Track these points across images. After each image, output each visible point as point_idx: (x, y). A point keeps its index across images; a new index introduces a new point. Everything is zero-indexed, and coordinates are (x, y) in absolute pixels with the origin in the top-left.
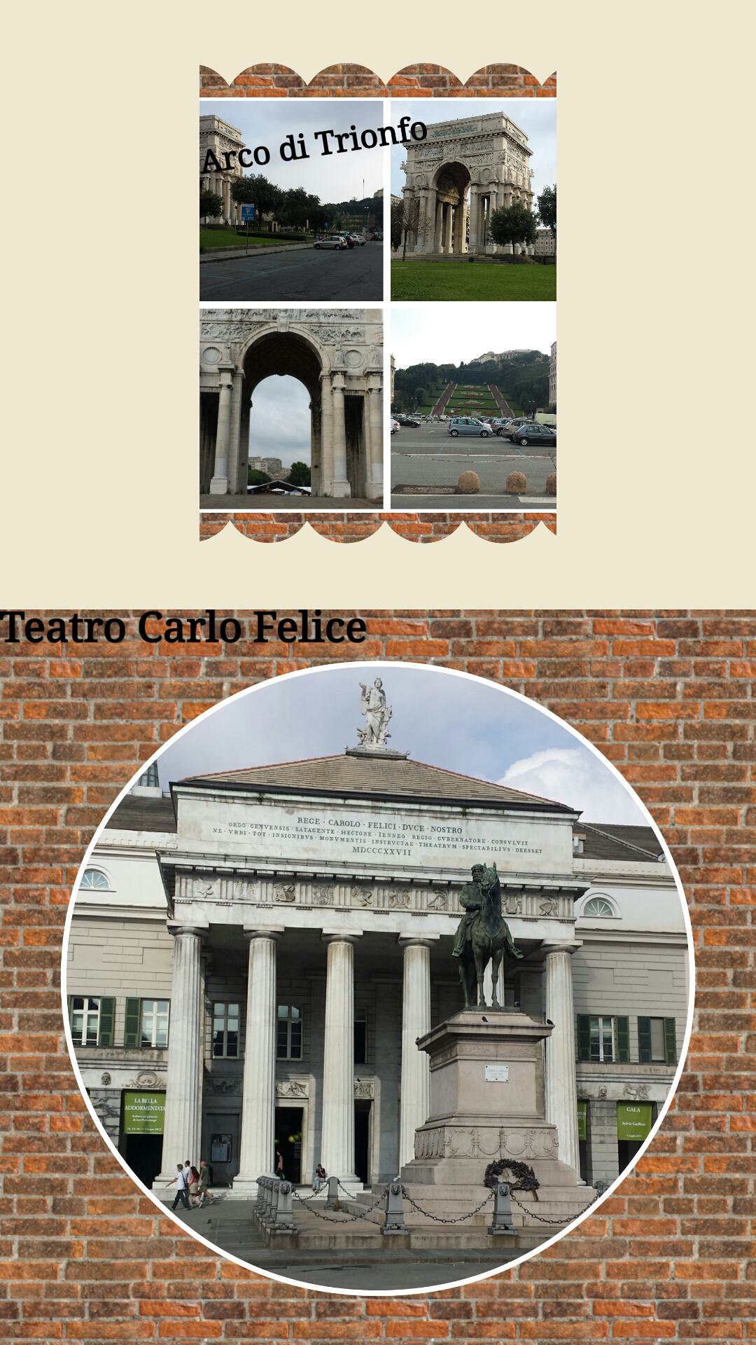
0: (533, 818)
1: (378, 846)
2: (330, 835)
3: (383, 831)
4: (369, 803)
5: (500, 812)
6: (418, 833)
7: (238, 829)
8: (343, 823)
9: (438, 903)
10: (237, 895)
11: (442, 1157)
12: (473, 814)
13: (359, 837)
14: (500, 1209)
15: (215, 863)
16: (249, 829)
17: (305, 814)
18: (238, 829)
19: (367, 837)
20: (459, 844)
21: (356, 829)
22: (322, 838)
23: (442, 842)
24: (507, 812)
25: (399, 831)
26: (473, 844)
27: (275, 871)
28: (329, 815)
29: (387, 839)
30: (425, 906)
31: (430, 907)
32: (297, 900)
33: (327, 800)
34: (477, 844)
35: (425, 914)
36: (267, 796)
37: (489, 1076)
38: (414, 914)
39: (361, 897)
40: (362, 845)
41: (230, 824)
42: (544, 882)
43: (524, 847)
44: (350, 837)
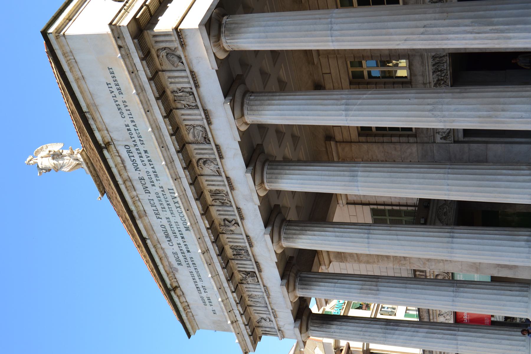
0: (77, 80)
4: (139, 222)
5: (88, 115)
7: (207, 301)
8: (167, 236)
9: (212, 166)
12: (103, 138)
15: (242, 326)
17: (172, 260)
18: (207, 301)
19: (172, 220)
20: (142, 148)
24: (85, 109)
25: (153, 196)
26: (135, 135)
28: (165, 244)
30: (219, 178)
31: (220, 175)
33: (153, 251)
34: (133, 131)
36: (169, 286)
38: (232, 188)
42: (144, 79)
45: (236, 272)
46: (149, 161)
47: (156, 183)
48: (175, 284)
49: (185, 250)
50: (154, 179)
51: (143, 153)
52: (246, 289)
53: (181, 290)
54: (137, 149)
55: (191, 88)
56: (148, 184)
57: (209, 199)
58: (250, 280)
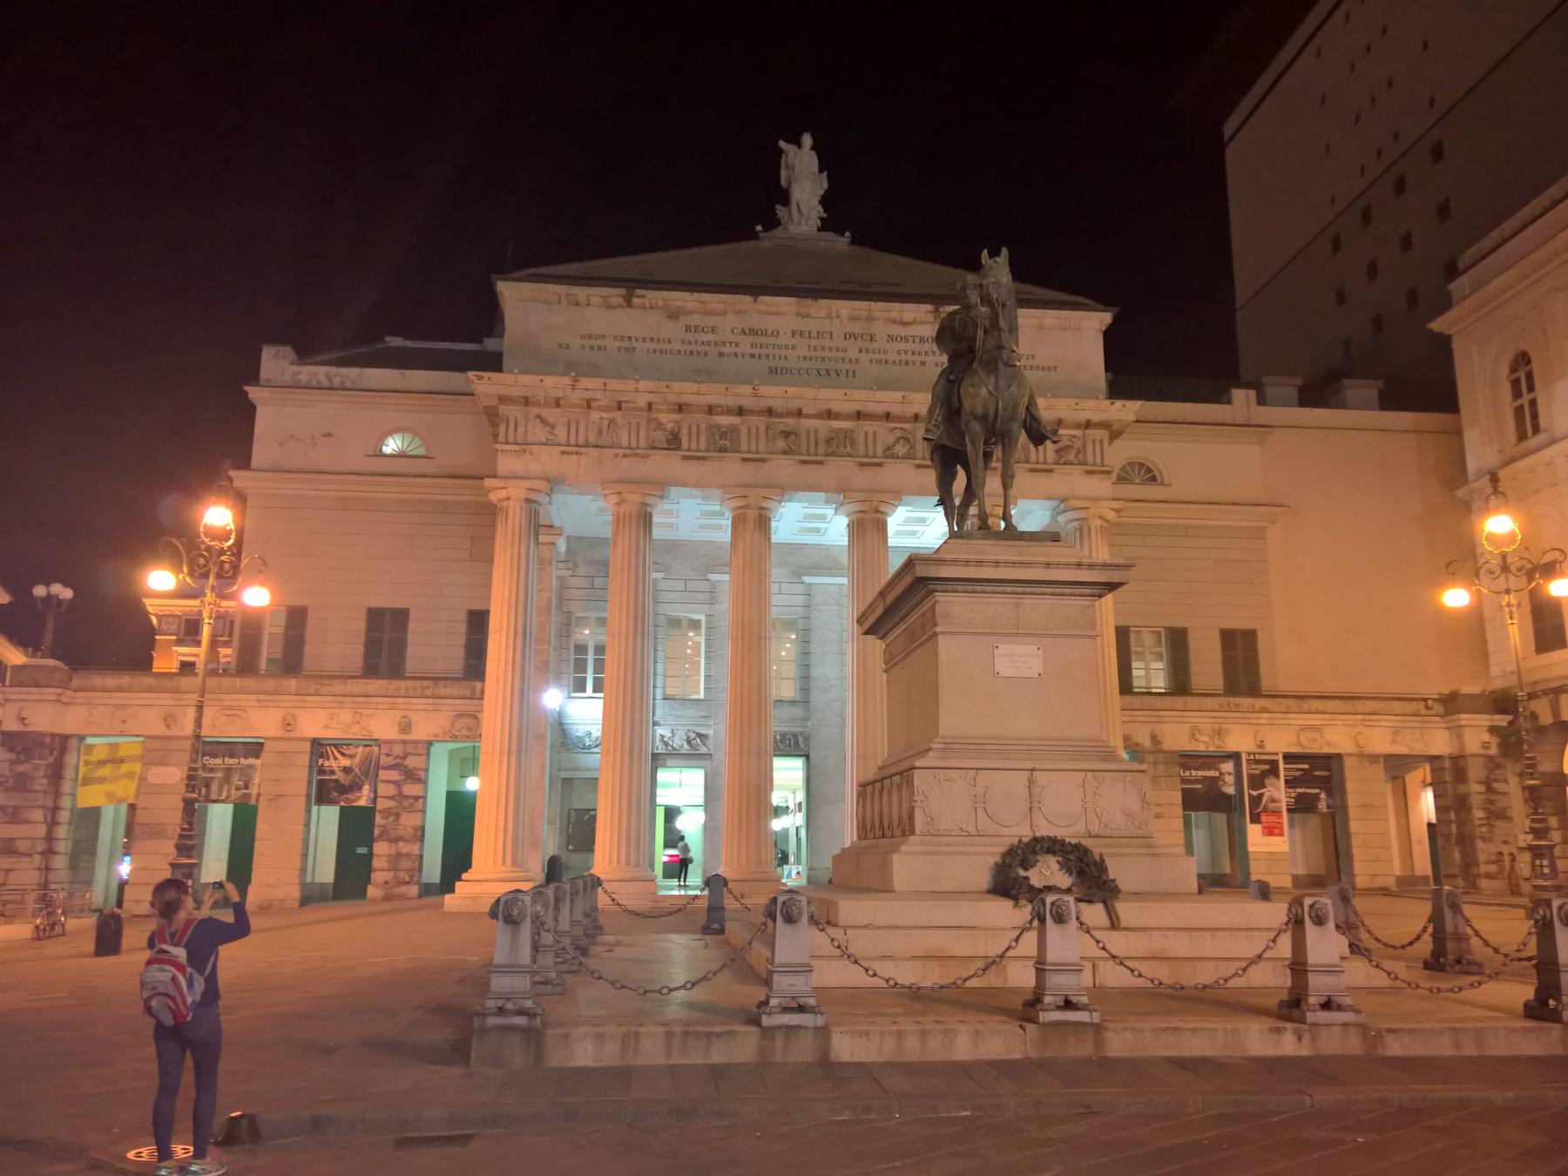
1: (806, 365)
2: (734, 350)
3: (815, 342)
6: (866, 344)
7: (595, 343)
8: (754, 332)
9: (901, 449)
10: (592, 439)
11: (913, 832)
13: (777, 352)
14: (1052, 955)
16: (611, 344)
19: (789, 353)
21: (772, 340)
22: (721, 354)
23: (904, 357)
27: (650, 405)
28: (731, 321)
29: (821, 354)
30: (879, 452)
32: (685, 444)
35: (880, 465)
37: (1002, 667)
38: (862, 465)
39: (781, 443)
40: (782, 363)
41: (583, 337)
44: (764, 351)
45: (678, 417)
46: (907, 363)
47: (863, 356)
48: (636, 301)
49: (726, 349)
50: (871, 356)
51: (922, 358)
52: (634, 422)
53: (620, 306)
54: (926, 353)
55: (1027, 461)
56: (860, 343)
58: (660, 437)
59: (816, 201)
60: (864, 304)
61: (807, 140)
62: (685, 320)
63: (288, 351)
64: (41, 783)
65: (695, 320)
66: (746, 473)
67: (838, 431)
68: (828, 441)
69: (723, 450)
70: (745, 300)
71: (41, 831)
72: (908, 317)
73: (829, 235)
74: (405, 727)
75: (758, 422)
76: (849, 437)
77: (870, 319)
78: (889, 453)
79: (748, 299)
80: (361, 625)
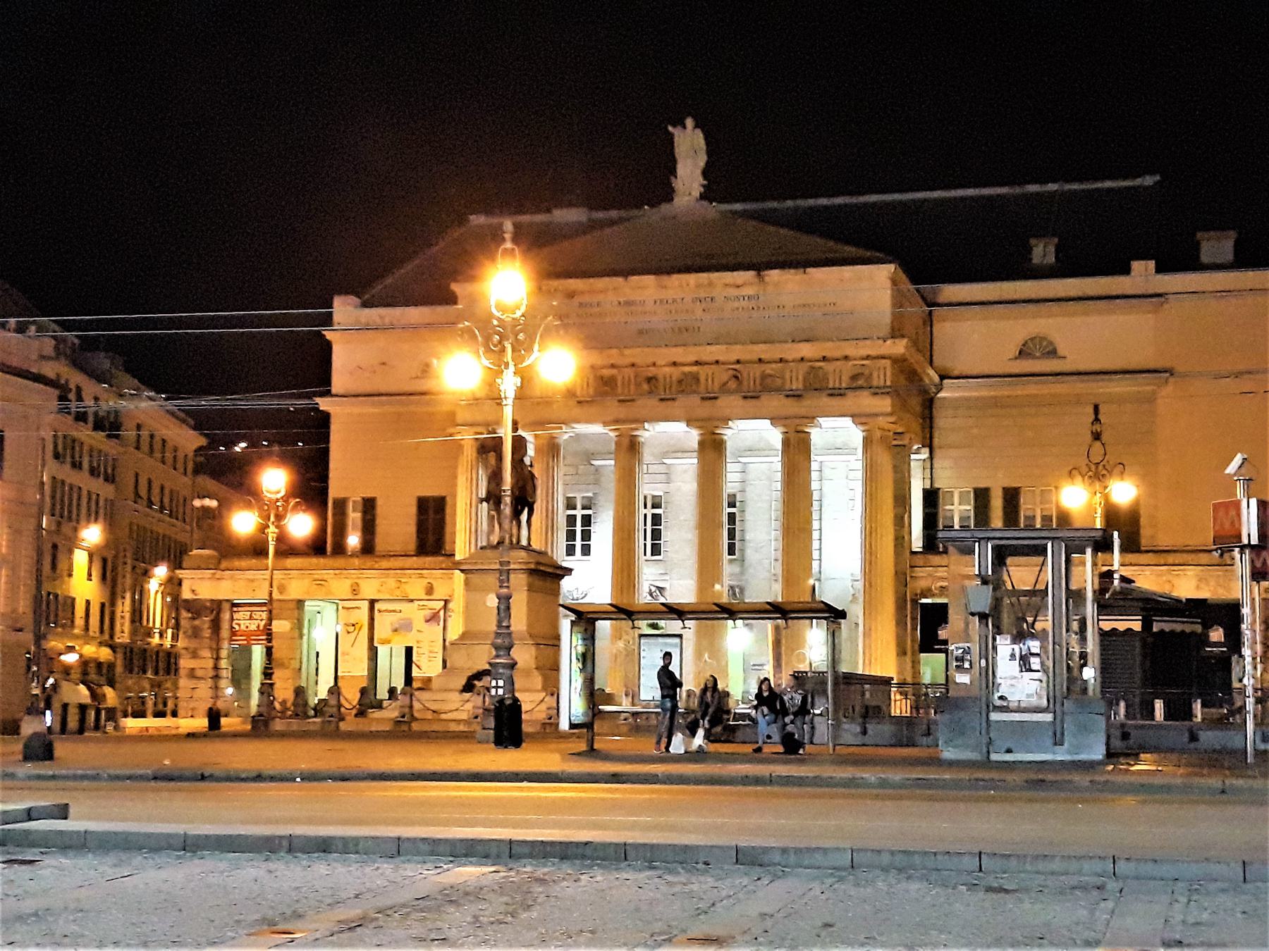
4: (652, 277)
9: (733, 385)
24: (808, 270)
28: (612, 298)
30: (716, 389)
39: (645, 387)
43: (832, 308)
57: (687, 369)
59: (699, 172)
60: (705, 275)
61: (689, 122)
62: (576, 300)
63: (353, 299)
64: (207, 633)
65: (586, 299)
66: (622, 412)
67: (684, 374)
68: (680, 382)
69: (605, 394)
70: (619, 280)
71: (210, 663)
72: (740, 282)
73: (705, 203)
74: (430, 590)
75: (629, 372)
76: (696, 378)
77: (711, 284)
78: (724, 389)
79: (620, 279)
80: (413, 510)
